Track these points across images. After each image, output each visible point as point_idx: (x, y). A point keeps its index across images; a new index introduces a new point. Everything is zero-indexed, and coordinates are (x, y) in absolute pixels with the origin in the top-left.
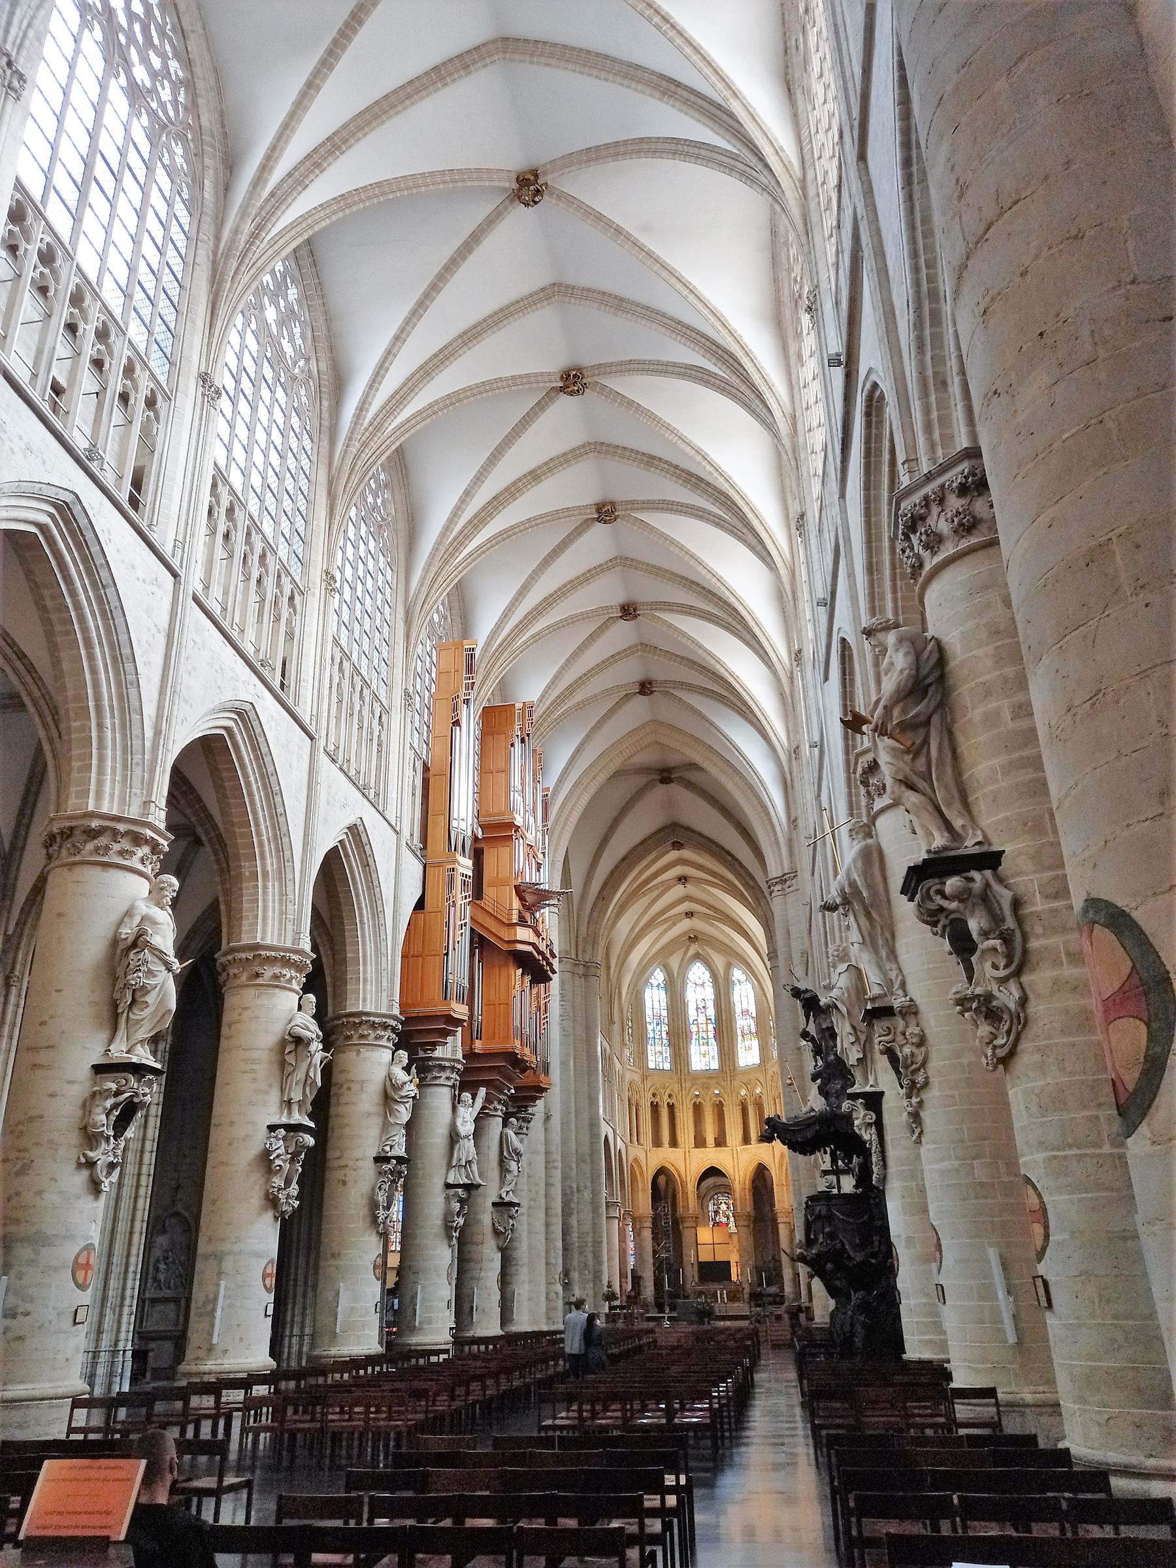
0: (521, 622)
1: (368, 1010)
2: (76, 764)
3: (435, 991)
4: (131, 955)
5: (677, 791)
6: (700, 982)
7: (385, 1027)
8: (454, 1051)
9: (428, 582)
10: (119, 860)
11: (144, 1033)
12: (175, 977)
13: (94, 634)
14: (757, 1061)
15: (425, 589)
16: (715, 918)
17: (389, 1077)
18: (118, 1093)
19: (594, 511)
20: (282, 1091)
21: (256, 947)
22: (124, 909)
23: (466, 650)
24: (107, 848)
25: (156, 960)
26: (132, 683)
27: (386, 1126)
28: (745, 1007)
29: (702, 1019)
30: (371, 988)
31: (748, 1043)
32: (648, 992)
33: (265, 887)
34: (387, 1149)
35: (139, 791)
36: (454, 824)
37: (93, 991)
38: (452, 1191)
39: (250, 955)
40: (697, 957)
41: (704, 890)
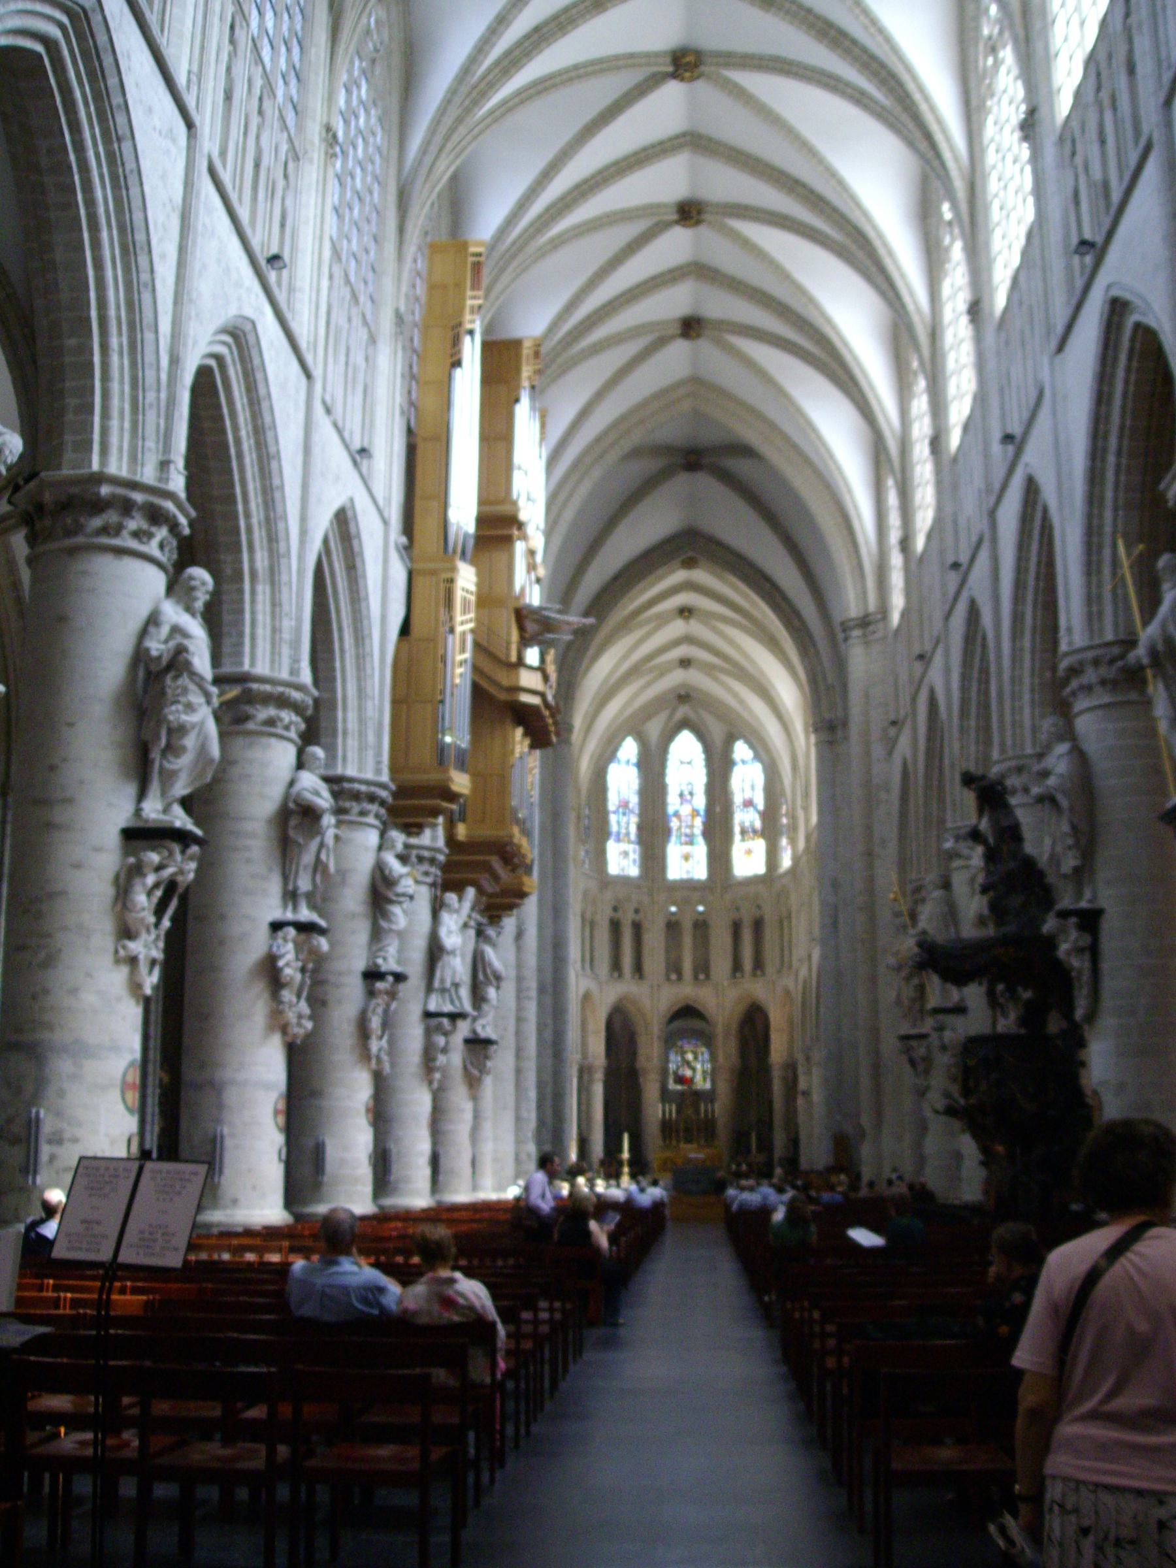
1: (351, 771)
2: (72, 402)
3: (425, 755)
5: (704, 482)
7: (372, 798)
8: (434, 838)
10: (134, 544)
13: (101, 210)
15: (428, 160)
16: (722, 670)
17: (380, 869)
18: (159, 868)
19: (668, 59)
20: (285, 877)
21: (243, 679)
22: (144, 613)
26: (146, 286)
27: (377, 934)
28: (748, 795)
29: (685, 810)
31: (749, 844)
33: (253, 592)
34: (380, 961)
38: (434, 1022)
40: (685, 724)
41: (714, 629)
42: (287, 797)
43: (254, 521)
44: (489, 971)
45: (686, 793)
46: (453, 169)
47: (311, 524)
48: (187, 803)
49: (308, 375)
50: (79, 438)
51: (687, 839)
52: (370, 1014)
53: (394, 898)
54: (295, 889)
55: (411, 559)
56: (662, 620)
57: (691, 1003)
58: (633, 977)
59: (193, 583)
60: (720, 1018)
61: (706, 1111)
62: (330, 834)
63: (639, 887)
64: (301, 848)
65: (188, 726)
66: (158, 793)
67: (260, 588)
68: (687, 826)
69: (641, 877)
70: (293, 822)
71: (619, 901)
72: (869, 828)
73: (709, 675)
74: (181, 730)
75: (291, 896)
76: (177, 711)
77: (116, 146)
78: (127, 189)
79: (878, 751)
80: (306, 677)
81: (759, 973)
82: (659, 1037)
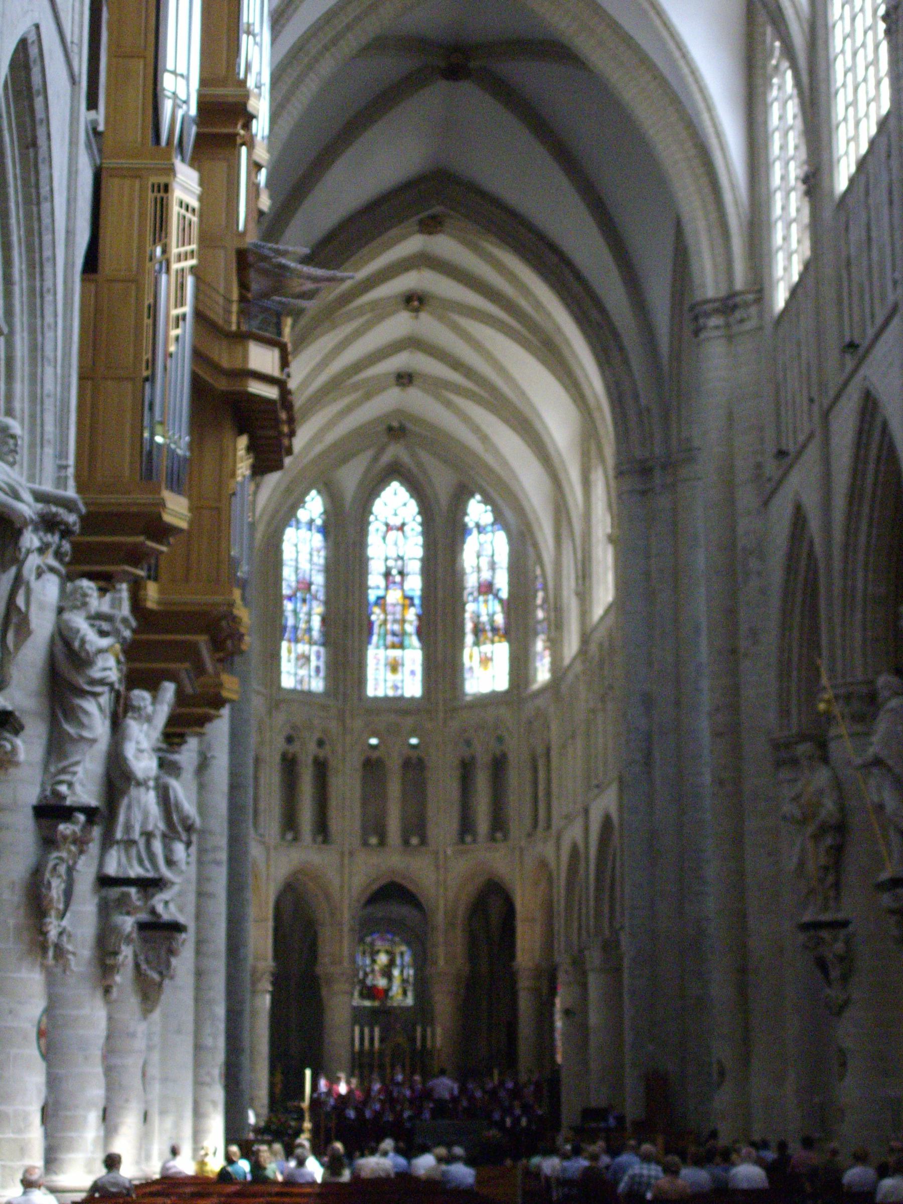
6: (397, 522)
14: (502, 684)
28: (486, 575)
29: (394, 596)
31: (486, 648)
32: (290, 534)
34: (63, 789)
36: (168, 82)
38: (115, 892)
40: (395, 471)
44: (175, 818)
45: (394, 572)
51: (396, 639)
52: (47, 875)
53: (87, 688)
55: (100, 151)
56: (381, 312)
57: (399, 880)
58: (314, 840)
60: (441, 903)
61: (424, 1038)
63: (324, 707)
68: (395, 621)
69: (327, 693)
71: (294, 728)
72: (731, 612)
73: (437, 397)
79: (747, 498)
81: (499, 835)
82: (352, 930)
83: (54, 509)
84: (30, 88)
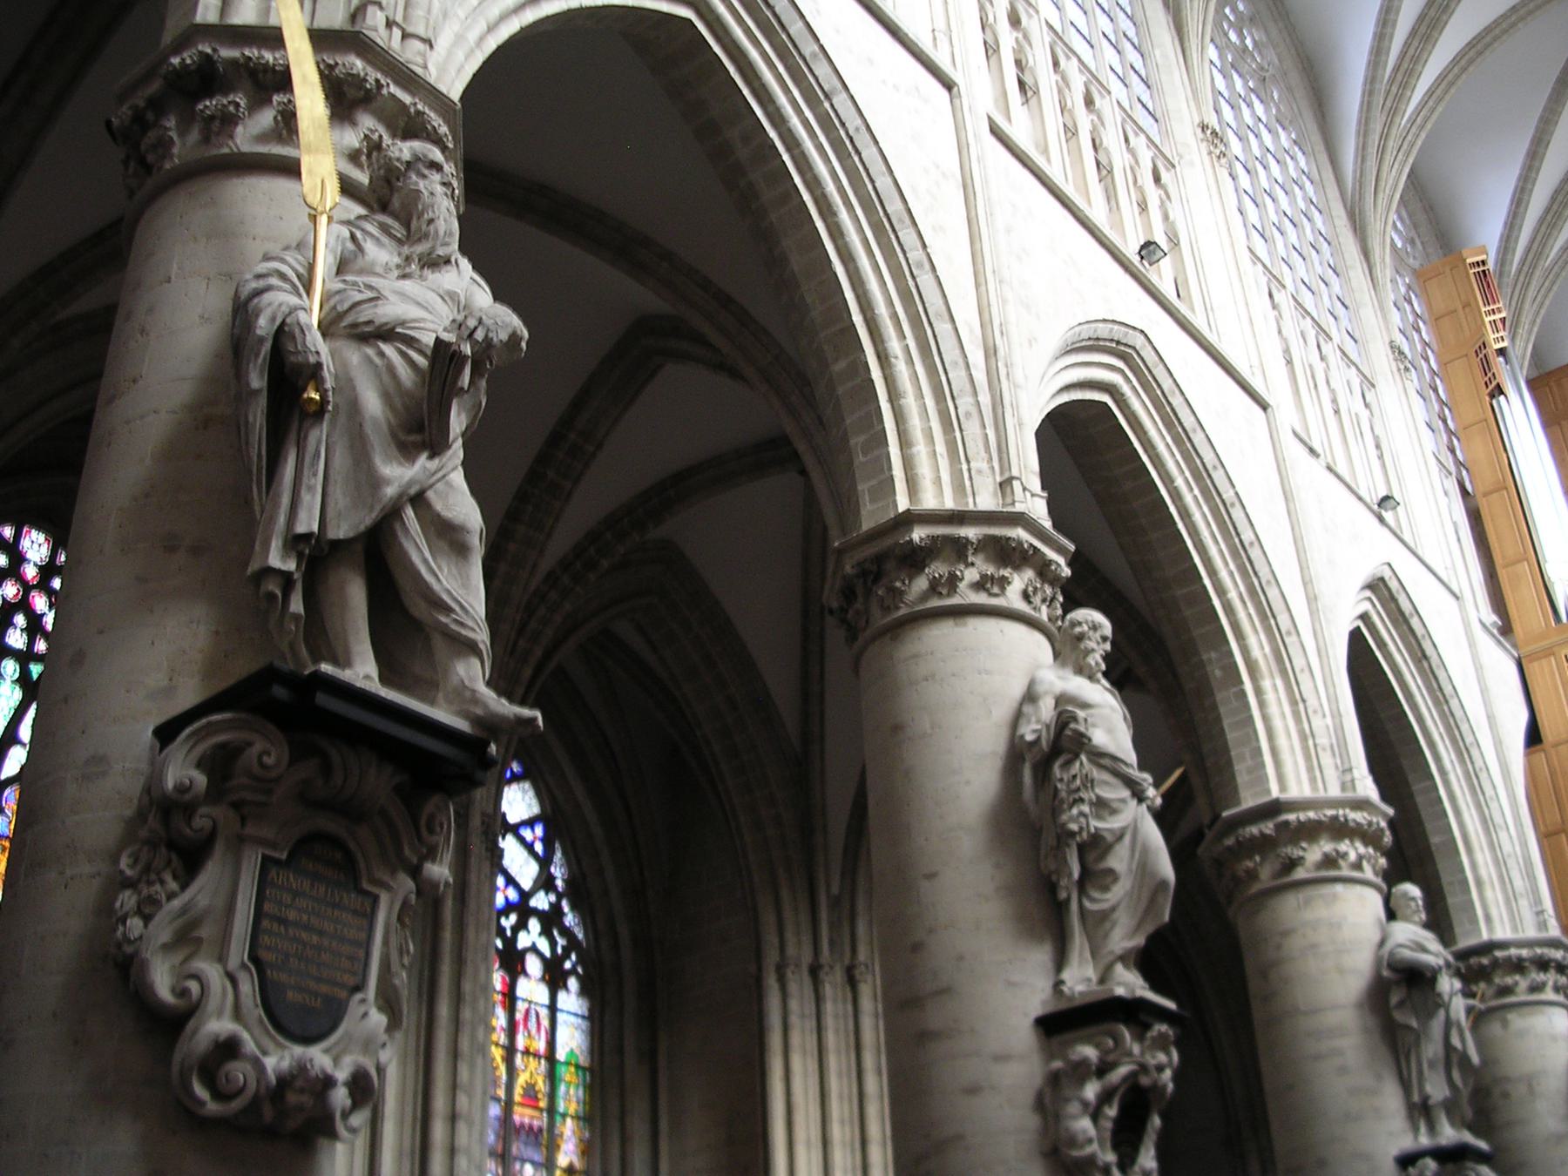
0: (1548, 210)
2: (857, 441)
4: (1057, 770)
7: (1543, 965)
9: (1372, 150)
10: (981, 598)
11: (1124, 937)
12: (1160, 816)
13: (831, 188)
20: (1406, 1085)
21: (1274, 809)
22: (1017, 690)
23: (1473, 265)
24: (953, 581)
25: (1106, 776)
26: (920, 265)
30: (1494, 895)
33: (1259, 692)
35: (984, 466)
37: (997, 866)
39: (1268, 827)
42: (1378, 962)
43: (1233, 595)
46: (1407, 170)
47: (1323, 587)
48: (1147, 961)
49: (1264, 406)
50: (874, 482)
54: (1425, 1099)
55: (1515, 646)
59: (1078, 630)
62: (1459, 1006)
64: (1418, 1037)
65: (1109, 838)
66: (1088, 954)
67: (1266, 684)
70: (1394, 999)
74: (1096, 846)
75: (1420, 1111)
76: (1082, 814)
77: (827, 105)
78: (858, 153)
80: (1367, 787)
83: (1539, 951)
84: (1402, 613)
